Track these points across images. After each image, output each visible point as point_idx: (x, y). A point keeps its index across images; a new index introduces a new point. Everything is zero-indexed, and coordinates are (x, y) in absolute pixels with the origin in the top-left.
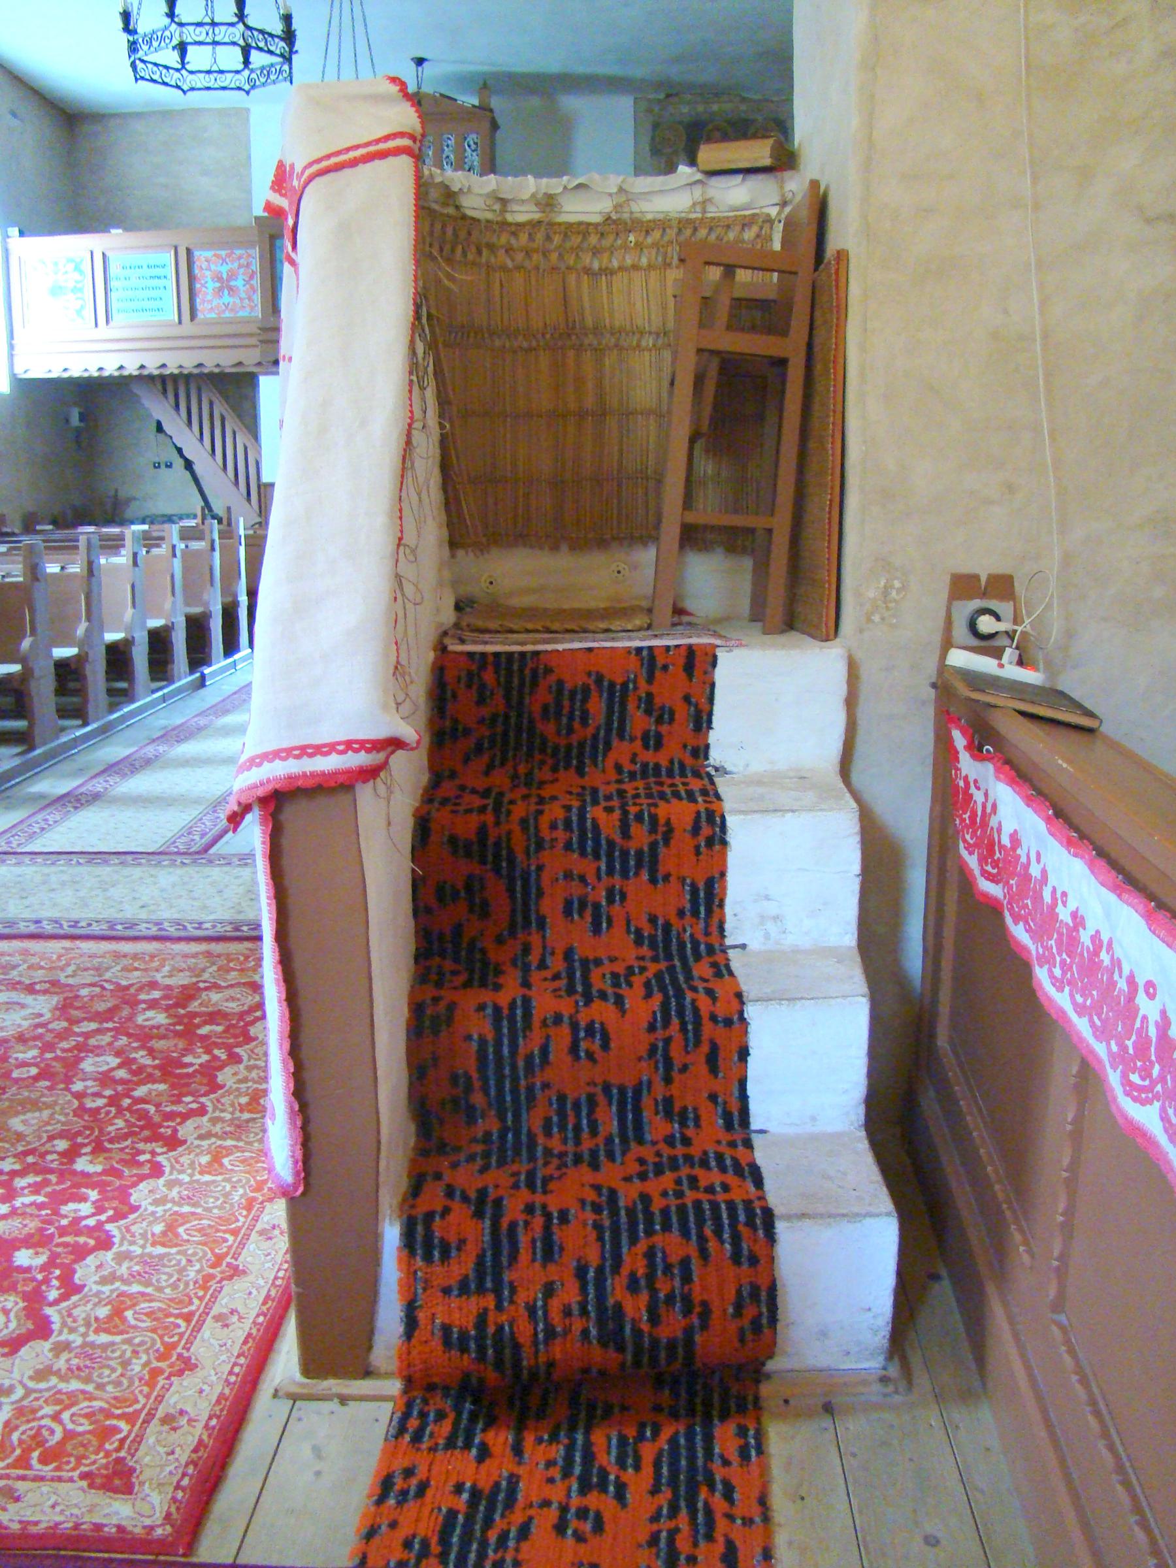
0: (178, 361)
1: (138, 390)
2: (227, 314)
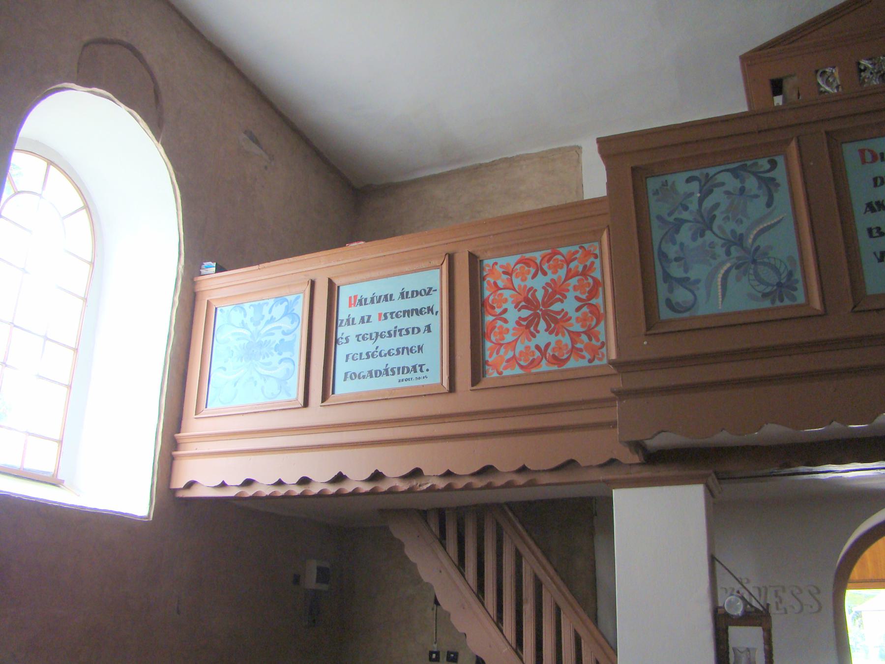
0: (441, 461)
1: (400, 531)
2: (544, 367)
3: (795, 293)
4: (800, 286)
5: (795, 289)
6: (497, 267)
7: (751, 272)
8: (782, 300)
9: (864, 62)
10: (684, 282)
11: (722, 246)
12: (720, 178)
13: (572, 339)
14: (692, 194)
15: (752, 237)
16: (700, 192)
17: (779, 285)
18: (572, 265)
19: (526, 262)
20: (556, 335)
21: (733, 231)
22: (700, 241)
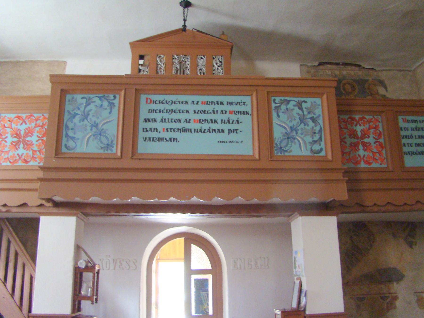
2: (20, 163)
3: (113, 149)
4: (115, 146)
5: (113, 147)
6: (6, 118)
7: (99, 138)
8: (107, 151)
9: (175, 56)
10: (73, 138)
11: (90, 126)
12: (94, 99)
13: (33, 153)
14: (82, 104)
15: (101, 125)
16: (86, 104)
17: (108, 145)
18: (38, 122)
19: (19, 117)
20: (27, 150)
21: (95, 122)
22: (82, 123)
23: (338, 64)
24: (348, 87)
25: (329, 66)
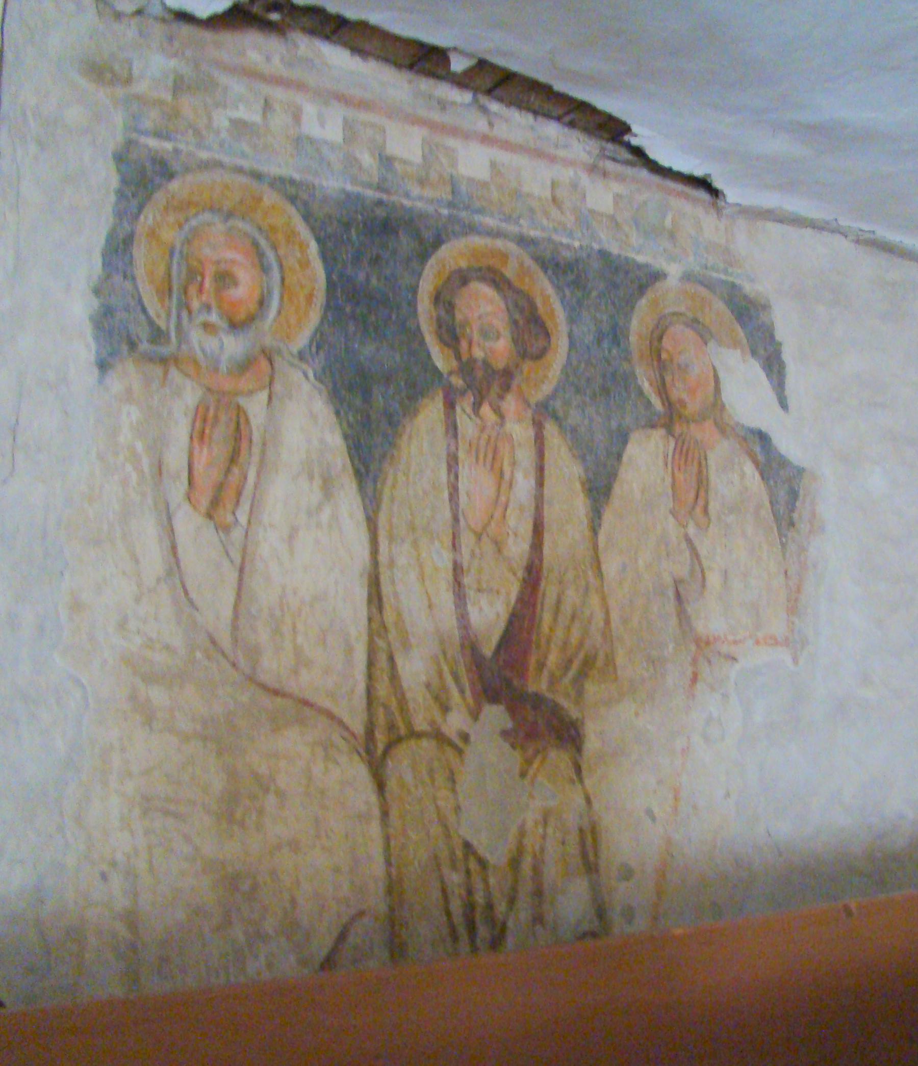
23: (425, 59)
24: (483, 306)
25: (336, 58)
